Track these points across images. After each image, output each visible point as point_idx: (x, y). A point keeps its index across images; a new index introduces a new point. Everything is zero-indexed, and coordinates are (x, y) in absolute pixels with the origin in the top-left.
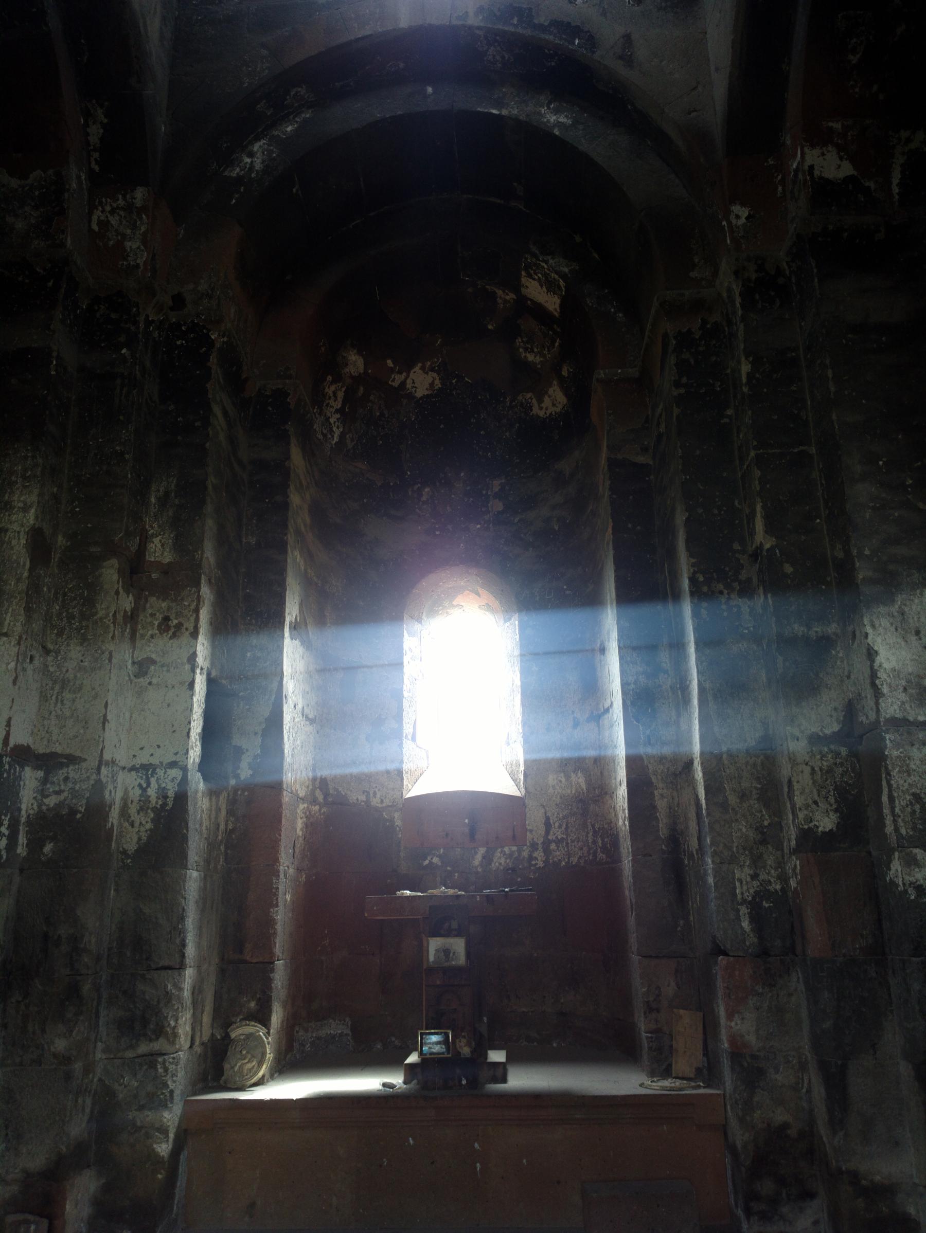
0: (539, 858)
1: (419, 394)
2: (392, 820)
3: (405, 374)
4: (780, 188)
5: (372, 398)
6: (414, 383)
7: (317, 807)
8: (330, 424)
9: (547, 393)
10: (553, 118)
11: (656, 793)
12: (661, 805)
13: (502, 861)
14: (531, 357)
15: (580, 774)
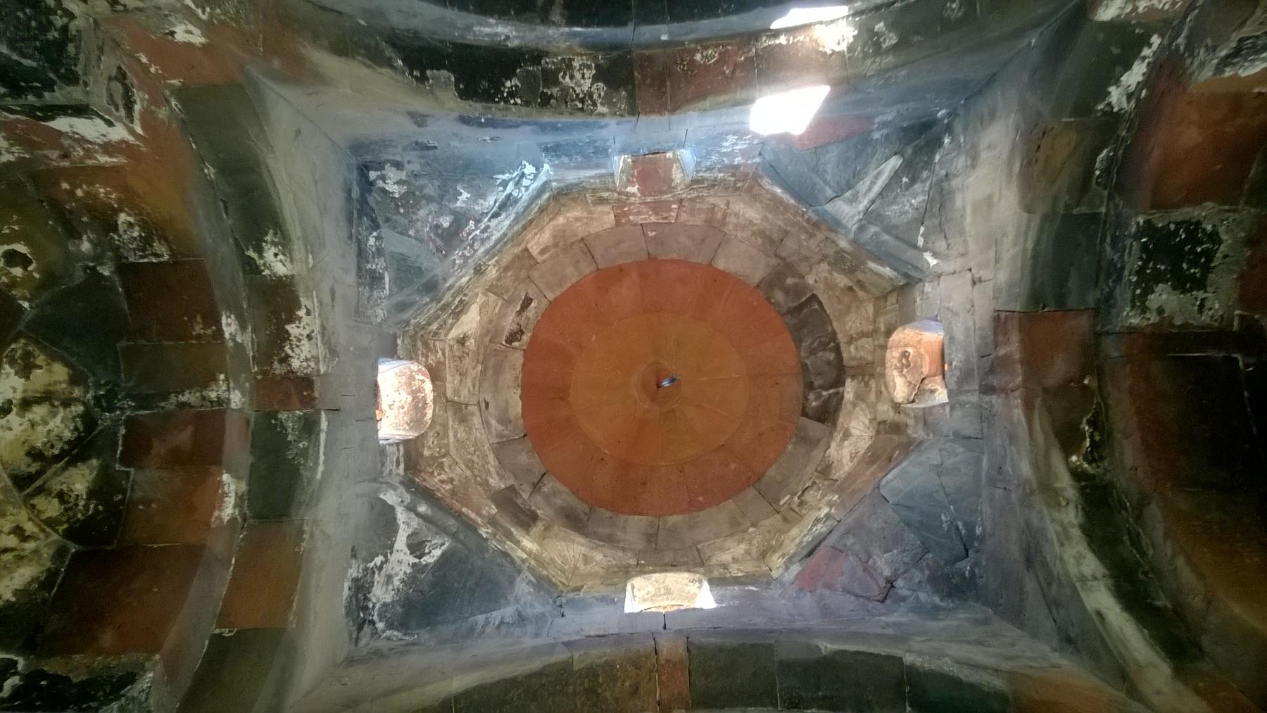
4: (144, 60)
10: (500, 29)
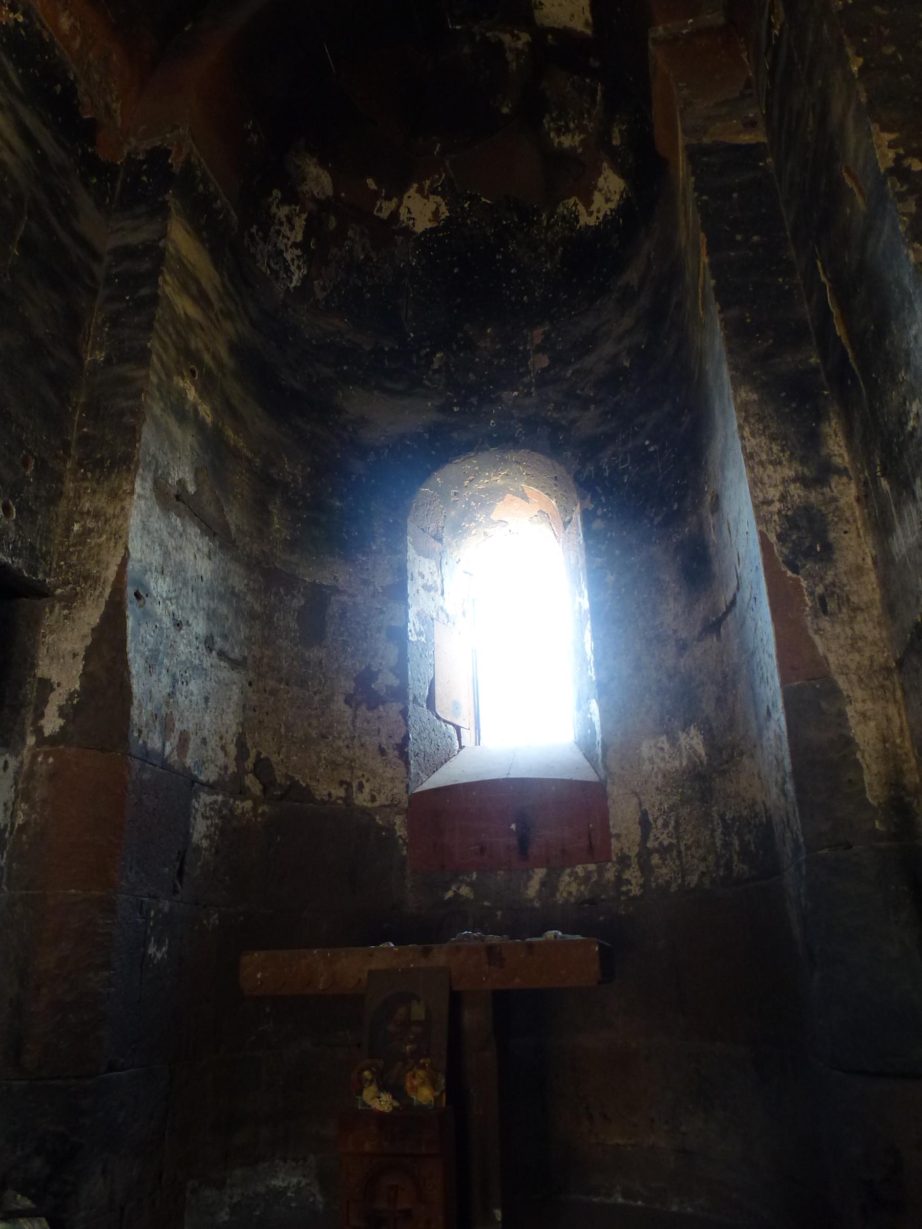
0: (634, 881)
1: (419, 228)
2: (391, 829)
3: (395, 200)
5: (350, 233)
6: (409, 212)
7: (248, 804)
8: (285, 260)
9: (595, 187)
11: (850, 710)
12: (864, 734)
13: (574, 888)
14: (567, 141)
15: (693, 731)
